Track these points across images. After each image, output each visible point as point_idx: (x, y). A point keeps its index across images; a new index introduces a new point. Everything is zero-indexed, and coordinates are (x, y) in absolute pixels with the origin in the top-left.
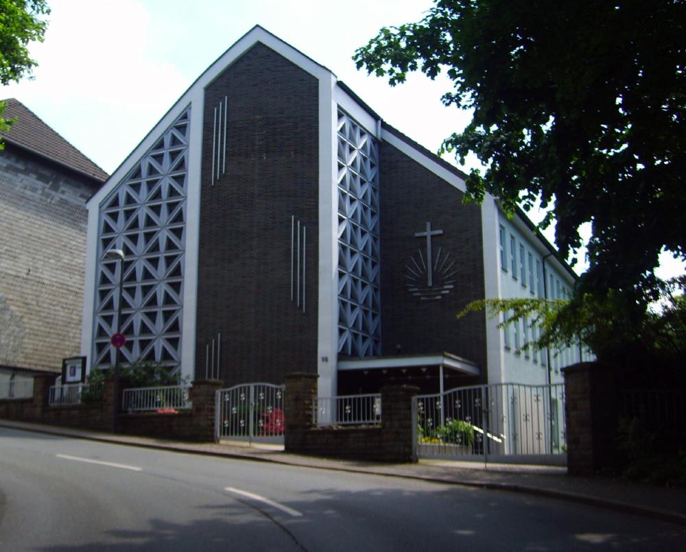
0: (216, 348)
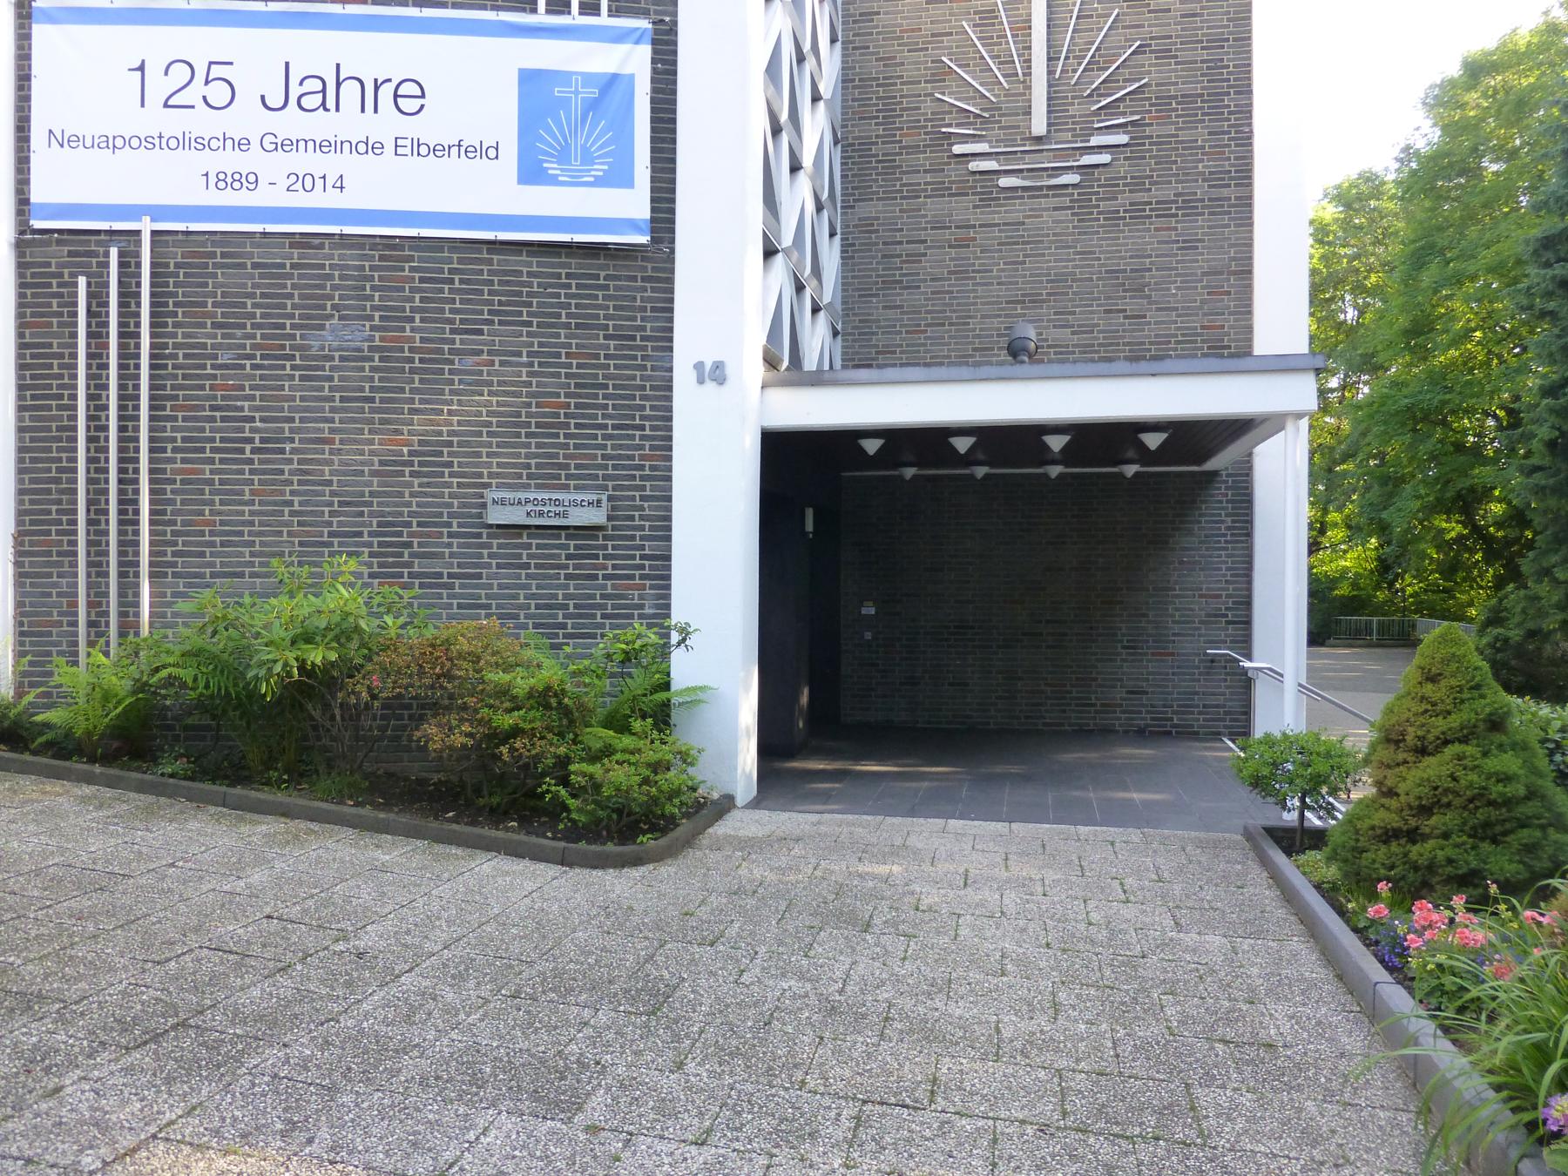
0: (129, 296)
